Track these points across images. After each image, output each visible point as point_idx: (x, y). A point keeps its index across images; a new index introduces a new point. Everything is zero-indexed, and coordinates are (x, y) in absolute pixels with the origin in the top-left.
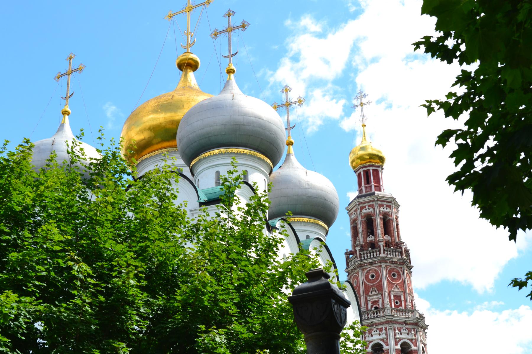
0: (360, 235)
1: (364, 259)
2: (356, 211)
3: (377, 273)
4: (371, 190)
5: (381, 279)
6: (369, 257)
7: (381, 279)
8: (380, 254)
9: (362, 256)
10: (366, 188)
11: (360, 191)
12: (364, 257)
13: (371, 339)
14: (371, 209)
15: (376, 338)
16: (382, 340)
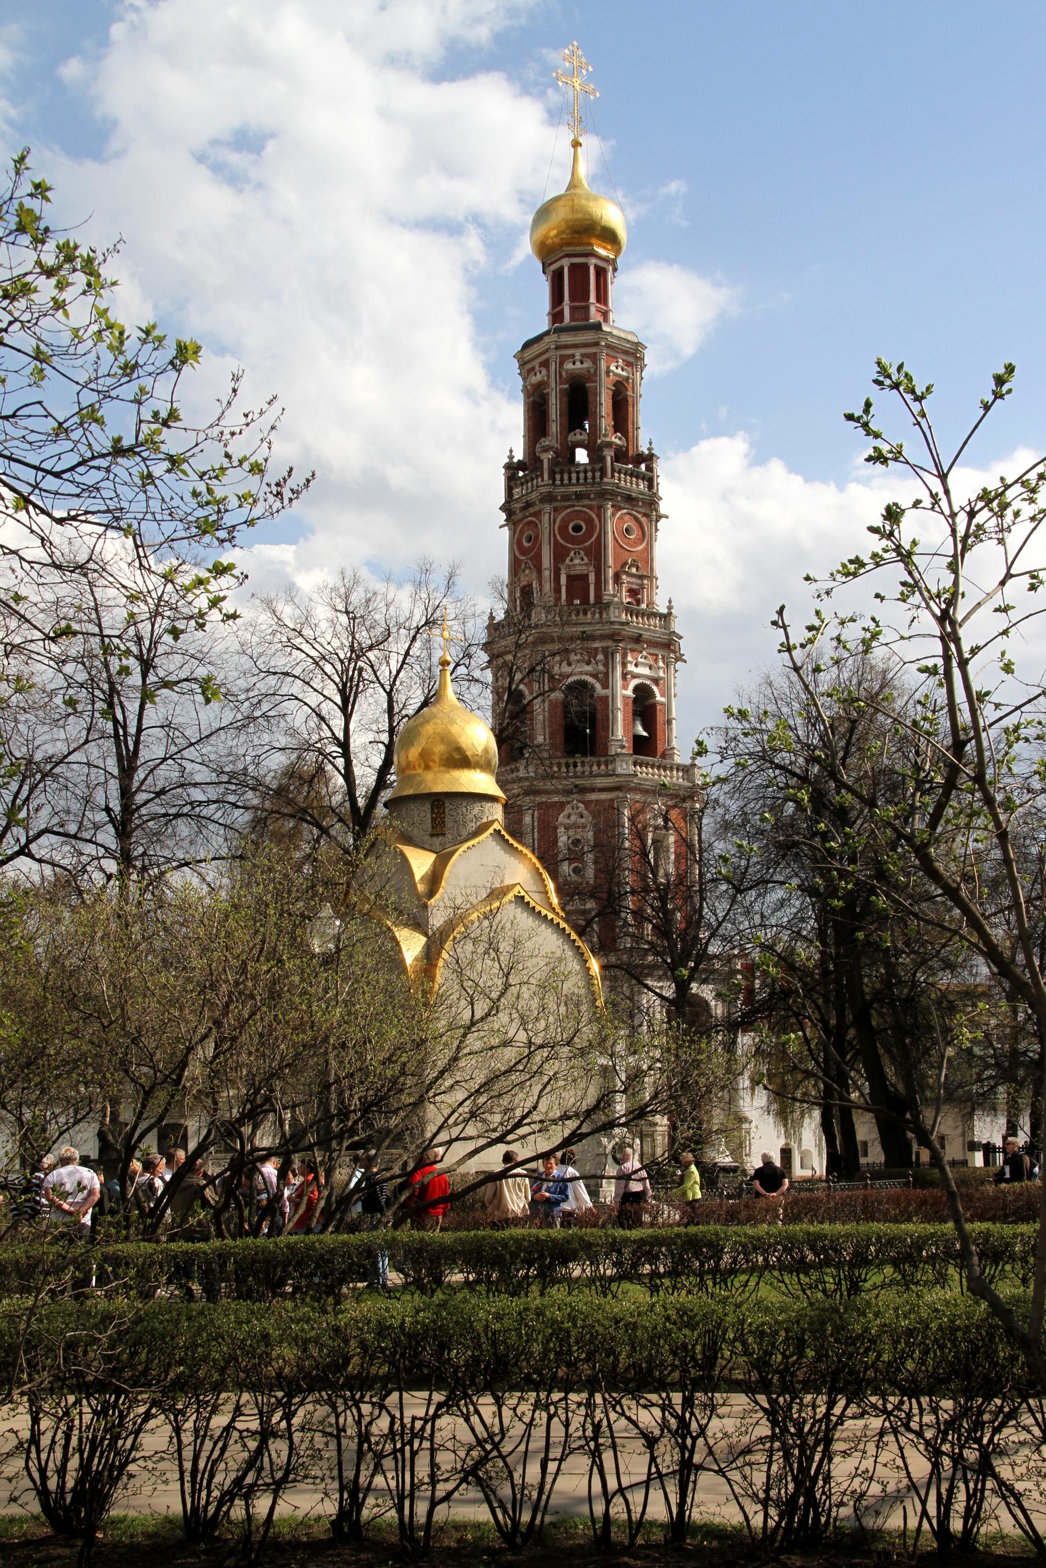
0: (554, 428)
1: (562, 485)
2: (545, 364)
3: (590, 522)
4: (587, 317)
5: (599, 538)
6: (574, 481)
7: (599, 538)
8: (601, 478)
9: (558, 477)
10: (572, 309)
11: (556, 316)
12: (562, 480)
13: (566, 669)
14: (588, 364)
15: (578, 671)
16: (595, 676)
